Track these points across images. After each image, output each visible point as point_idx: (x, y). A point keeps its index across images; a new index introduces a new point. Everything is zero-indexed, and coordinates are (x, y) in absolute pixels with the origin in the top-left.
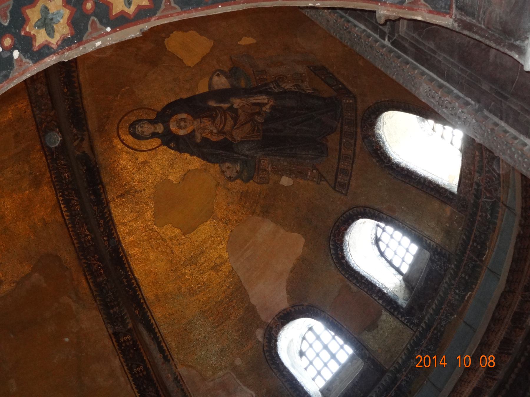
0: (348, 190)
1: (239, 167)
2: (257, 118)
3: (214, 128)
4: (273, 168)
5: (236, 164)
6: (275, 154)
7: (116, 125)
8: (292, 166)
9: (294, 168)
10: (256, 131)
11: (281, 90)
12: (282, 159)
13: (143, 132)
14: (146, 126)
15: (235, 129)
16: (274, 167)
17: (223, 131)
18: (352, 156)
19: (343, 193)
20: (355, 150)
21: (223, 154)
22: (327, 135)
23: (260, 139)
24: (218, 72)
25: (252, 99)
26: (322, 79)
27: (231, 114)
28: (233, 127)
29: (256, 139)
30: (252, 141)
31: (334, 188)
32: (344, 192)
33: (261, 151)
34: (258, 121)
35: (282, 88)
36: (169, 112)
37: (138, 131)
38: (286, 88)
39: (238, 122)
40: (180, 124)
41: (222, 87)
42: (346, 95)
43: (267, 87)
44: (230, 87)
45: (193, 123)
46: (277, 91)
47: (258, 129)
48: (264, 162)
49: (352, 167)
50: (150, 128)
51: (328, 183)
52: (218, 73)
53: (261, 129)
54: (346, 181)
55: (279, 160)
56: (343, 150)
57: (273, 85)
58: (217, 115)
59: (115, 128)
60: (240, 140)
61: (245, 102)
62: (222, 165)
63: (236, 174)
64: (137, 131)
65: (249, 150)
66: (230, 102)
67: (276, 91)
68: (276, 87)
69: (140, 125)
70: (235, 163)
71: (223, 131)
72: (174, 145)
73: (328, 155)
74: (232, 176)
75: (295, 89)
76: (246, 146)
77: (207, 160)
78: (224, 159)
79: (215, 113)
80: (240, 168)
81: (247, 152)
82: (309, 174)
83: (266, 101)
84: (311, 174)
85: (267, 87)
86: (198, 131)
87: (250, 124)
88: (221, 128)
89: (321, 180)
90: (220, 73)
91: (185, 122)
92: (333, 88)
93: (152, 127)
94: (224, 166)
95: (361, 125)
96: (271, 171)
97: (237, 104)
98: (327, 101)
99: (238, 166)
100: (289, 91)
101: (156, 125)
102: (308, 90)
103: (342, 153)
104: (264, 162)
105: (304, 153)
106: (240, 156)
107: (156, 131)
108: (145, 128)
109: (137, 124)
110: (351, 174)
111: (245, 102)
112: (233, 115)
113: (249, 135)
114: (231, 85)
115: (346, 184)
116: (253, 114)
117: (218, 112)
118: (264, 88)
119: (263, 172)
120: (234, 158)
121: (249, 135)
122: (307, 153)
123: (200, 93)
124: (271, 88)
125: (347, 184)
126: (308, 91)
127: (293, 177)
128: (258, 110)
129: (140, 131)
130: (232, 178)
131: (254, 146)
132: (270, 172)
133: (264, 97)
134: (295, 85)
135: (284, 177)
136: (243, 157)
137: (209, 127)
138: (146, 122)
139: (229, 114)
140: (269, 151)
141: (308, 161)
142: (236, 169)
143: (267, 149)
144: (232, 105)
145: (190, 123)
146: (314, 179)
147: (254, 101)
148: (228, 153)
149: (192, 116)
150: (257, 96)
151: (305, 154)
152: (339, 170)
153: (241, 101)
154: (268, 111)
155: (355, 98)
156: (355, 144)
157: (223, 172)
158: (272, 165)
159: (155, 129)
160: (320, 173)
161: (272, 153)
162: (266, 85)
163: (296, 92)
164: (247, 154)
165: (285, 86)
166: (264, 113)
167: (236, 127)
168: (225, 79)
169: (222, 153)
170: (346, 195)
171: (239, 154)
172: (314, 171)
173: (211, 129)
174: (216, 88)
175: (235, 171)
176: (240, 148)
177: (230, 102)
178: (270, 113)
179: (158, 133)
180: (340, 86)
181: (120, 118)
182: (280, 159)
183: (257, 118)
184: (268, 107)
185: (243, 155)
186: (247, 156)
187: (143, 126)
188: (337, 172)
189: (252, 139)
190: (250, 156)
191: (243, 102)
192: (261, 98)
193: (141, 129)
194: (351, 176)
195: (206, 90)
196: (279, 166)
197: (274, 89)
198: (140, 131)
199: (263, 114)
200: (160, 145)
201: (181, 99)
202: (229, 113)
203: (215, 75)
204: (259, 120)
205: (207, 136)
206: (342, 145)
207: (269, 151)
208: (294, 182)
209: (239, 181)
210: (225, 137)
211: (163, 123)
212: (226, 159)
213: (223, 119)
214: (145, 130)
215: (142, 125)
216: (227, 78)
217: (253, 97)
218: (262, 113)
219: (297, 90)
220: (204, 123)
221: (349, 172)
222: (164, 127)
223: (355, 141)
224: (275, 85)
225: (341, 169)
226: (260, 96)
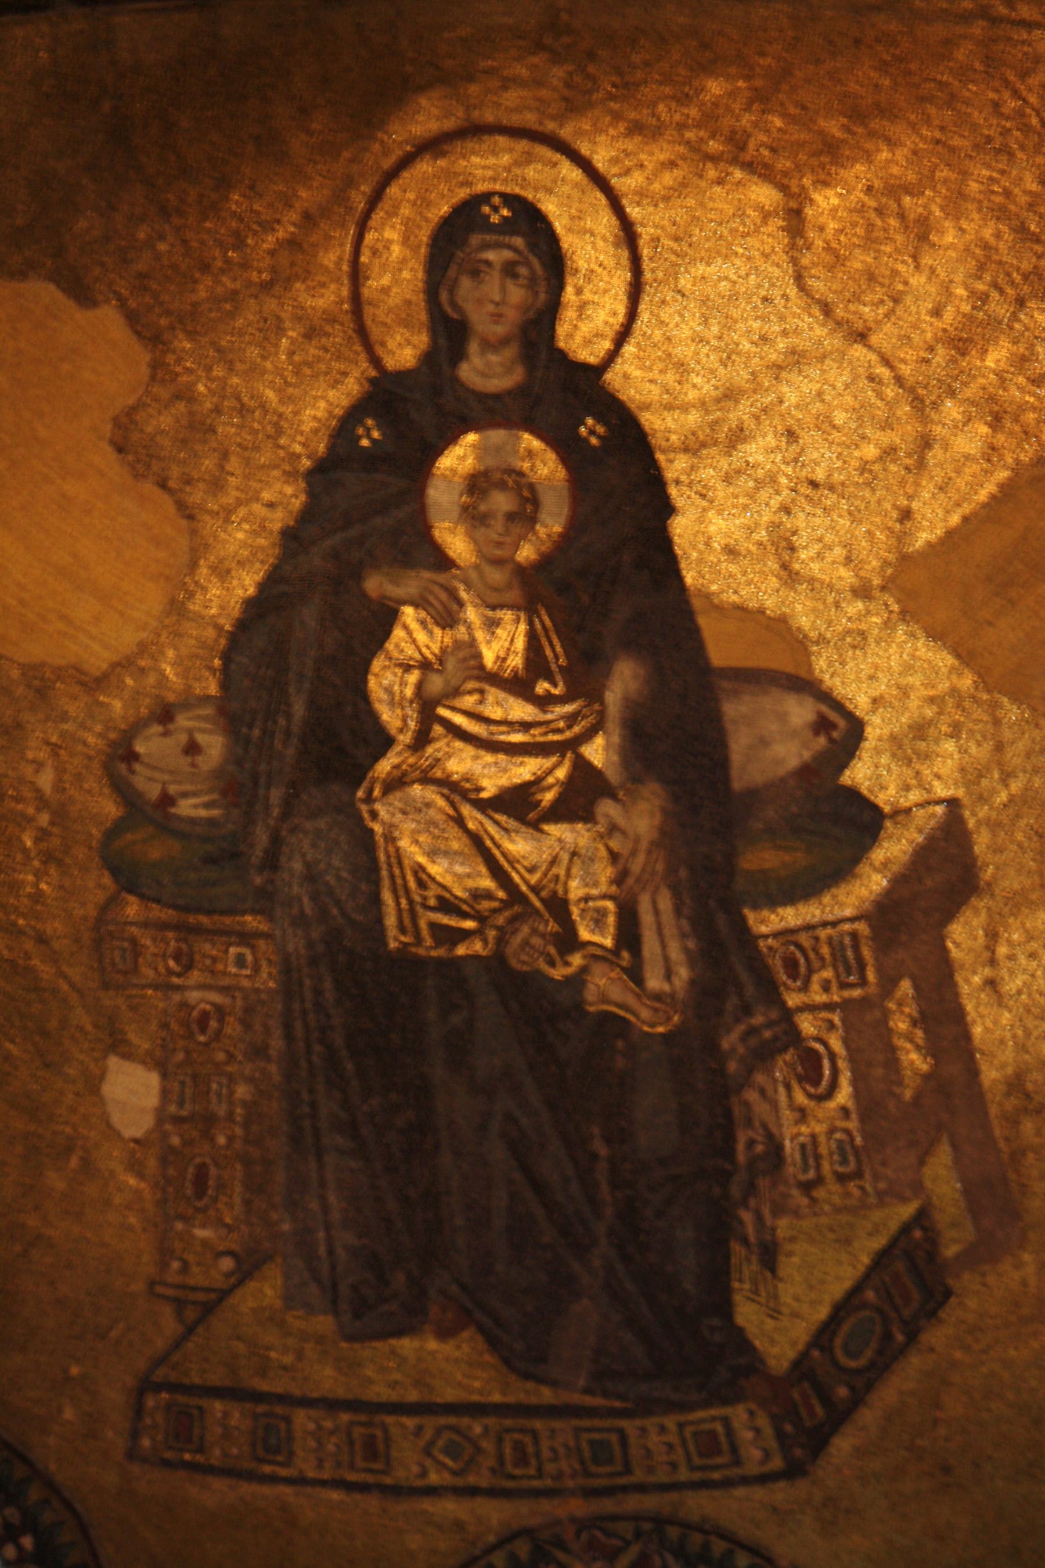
0: (167, 1464)
1: (203, 813)
2: (534, 931)
3: (454, 682)
4: (205, 1017)
5: (215, 796)
6: (298, 1025)
7: (550, 126)
8: (239, 1131)
9: (222, 1140)
10: (446, 920)
11: (732, 1066)
12: (273, 1068)
13: (475, 274)
14: (516, 294)
15: (453, 805)
16: (213, 1024)
17: (438, 729)
18: (388, 1481)
19: (135, 1435)
20: (432, 1491)
21: (282, 721)
22: (482, 1329)
23: (393, 945)
24: (842, 723)
25: (665, 903)
26: (857, 1290)
27: (551, 780)
28: (464, 795)
29: (391, 921)
30: (376, 900)
31: (146, 1386)
32: (146, 1443)
33: (310, 945)
34: (515, 932)
35: (750, 1071)
36: (592, 432)
37: (486, 246)
38: (751, 1095)
39: (498, 817)
40: (502, 486)
41: (739, 744)
42: (789, 1428)
43: (750, 991)
44: (737, 785)
45: (498, 562)
46: (725, 1045)
47: (465, 935)
48: (240, 961)
49: (323, 1483)
50: (497, 317)
51: (177, 1345)
52: (834, 726)
53: (461, 950)
54: (217, 1452)
55: (259, 1051)
56: (410, 1422)
57: (770, 1024)
58: (544, 702)
59: (529, 119)
60: (377, 828)
61: (636, 866)
62: (208, 711)
63: (153, 792)
64: (488, 237)
65: (311, 877)
66: (636, 780)
67: (730, 1041)
68: (753, 1041)
69: (528, 264)
70: (224, 794)
71: (438, 729)
72: (365, 442)
73: (351, 1338)
74: (137, 767)
75: (751, 1144)
76: (336, 862)
77: (243, 625)
78: (250, 726)
79: (556, 692)
80: (193, 821)
81: (297, 866)
82: (201, 1233)
83: (654, 982)
84: (205, 1243)
85: (750, 991)
86: (436, 589)
87: (487, 883)
88: (459, 719)
89: (179, 1304)
90: (835, 734)
91: (511, 517)
92: (816, 1353)
93: (500, 330)
94: (203, 725)
95: (615, 1518)
96: (184, 1005)
97: (621, 821)
98: (716, 1322)
99: (207, 806)
100: (728, 1115)
101: (510, 352)
102: (759, 1218)
103: (389, 1420)
104: (240, 961)
105: (332, 1198)
106: (272, 822)
107: (473, 347)
108: (503, 289)
109: (533, 247)
110: (273, 1479)
111: (636, 866)
112: (549, 797)
113: (412, 884)
114: (753, 795)
115: (200, 1450)
116: (559, 906)
117: (569, 708)
118: (744, 976)
119: (177, 958)
120: (256, 784)
121: (412, 884)
122: (336, 1216)
123: (702, 621)
124: (747, 1010)
125: (199, 1458)
126: (747, 1216)
127: (165, 1135)
128: (585, 934)
129: (491, 255)
130: (122, 767)
131: (343, 913)
132: (177, 997)
133: (683, 973)
134: (779, 1148)
135: (154, 1079)
136: (262, 838)
137: (461, 655)
138: (542, 296)
139: (550, 771)
140: (318, 992)
141: (286, 1227)
142: (185, 795)
143: (328, 985)
144: (614, 797)
145: (499, 545)
146: (176, 1265)
147: (647, 918)
148: (291, 752)
149: (544, 563)
150: (683, 936)
151: (325, 1209)
152: (279, 1410)
153: (644, 845)
154: (590, 994)
155: (793, 1471)
156: (473, 1492)
157: (165, 715)
158: (219, 1009)
159: (488, 346)
160: (224, 1294)
161: (304, 1012)
162: (771, 993)
163: (729, 1153)
164: (283, 859)
165: (762, 1092)
166: (569, 971)
167: (466, 810)
168: (793, 763)
169: (288, 716)
170: (131, 1455)
171: (285, 816)
172: (227, 1264)
173: (451, 664)
174: (732, 709)
175: (172, 789)
176: (322, 823)
177: (636, 780)
178: (579, 1006)
179: (458, 354)
180: (843, 1392)
181: (585, 149)
182: (269, 1059)
183: (534, 931)
184: (616, 993)
185: (276, 840)
186: (272, 862)
187: (515, 276)
188: (258, 1397)
189: (387, 896)
190: (272, 882)
191: (641, 858)
192: (675, 953)
193: (498, 267)
194: (251, 1476)
195: (718, 655)
196: (221, 1056)
197: (742, 1027)
198: (491, 255)
199: (567, 964)
200: (376, 361)
201: (668, 509)
202: (561, 773)
203: (824, 709)
204: (517, 940)
205: (398, 633)
206: (443, 1421)
207: (318, 992)
208: (136, 1141)
209: (111, 809)
210: (387, 742)
211: (520, 392)
212: (248, 741)
213: (517, 738)
214: (492, 285)
215: (523, 271)
216: (805, 772)
217: (678, 911)
218: (577, 960)
219: (741, 1157)
220: (492, 625)
221: (281, 1464)
222: (497, 397)
223: (492, 1493)
224: (767, 1034)
225: (288, 1420)
226: (686, 950)
